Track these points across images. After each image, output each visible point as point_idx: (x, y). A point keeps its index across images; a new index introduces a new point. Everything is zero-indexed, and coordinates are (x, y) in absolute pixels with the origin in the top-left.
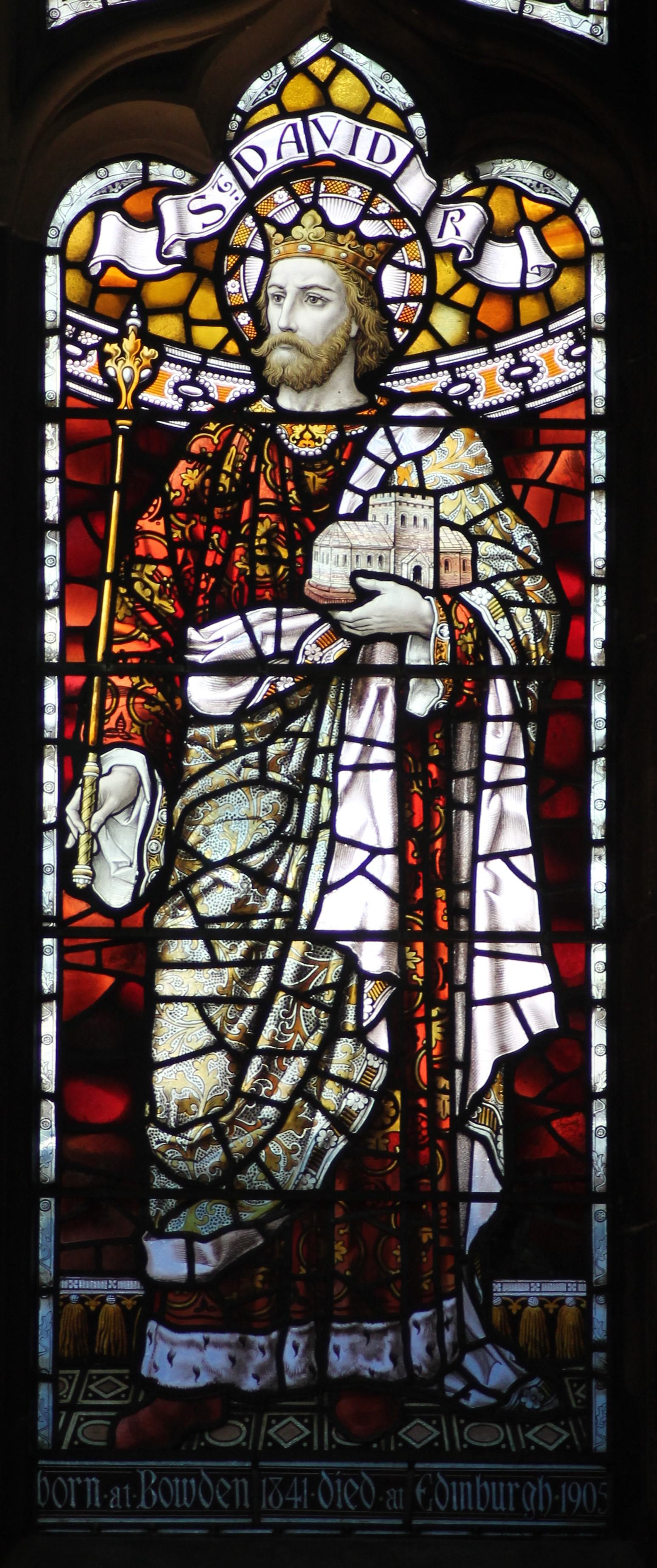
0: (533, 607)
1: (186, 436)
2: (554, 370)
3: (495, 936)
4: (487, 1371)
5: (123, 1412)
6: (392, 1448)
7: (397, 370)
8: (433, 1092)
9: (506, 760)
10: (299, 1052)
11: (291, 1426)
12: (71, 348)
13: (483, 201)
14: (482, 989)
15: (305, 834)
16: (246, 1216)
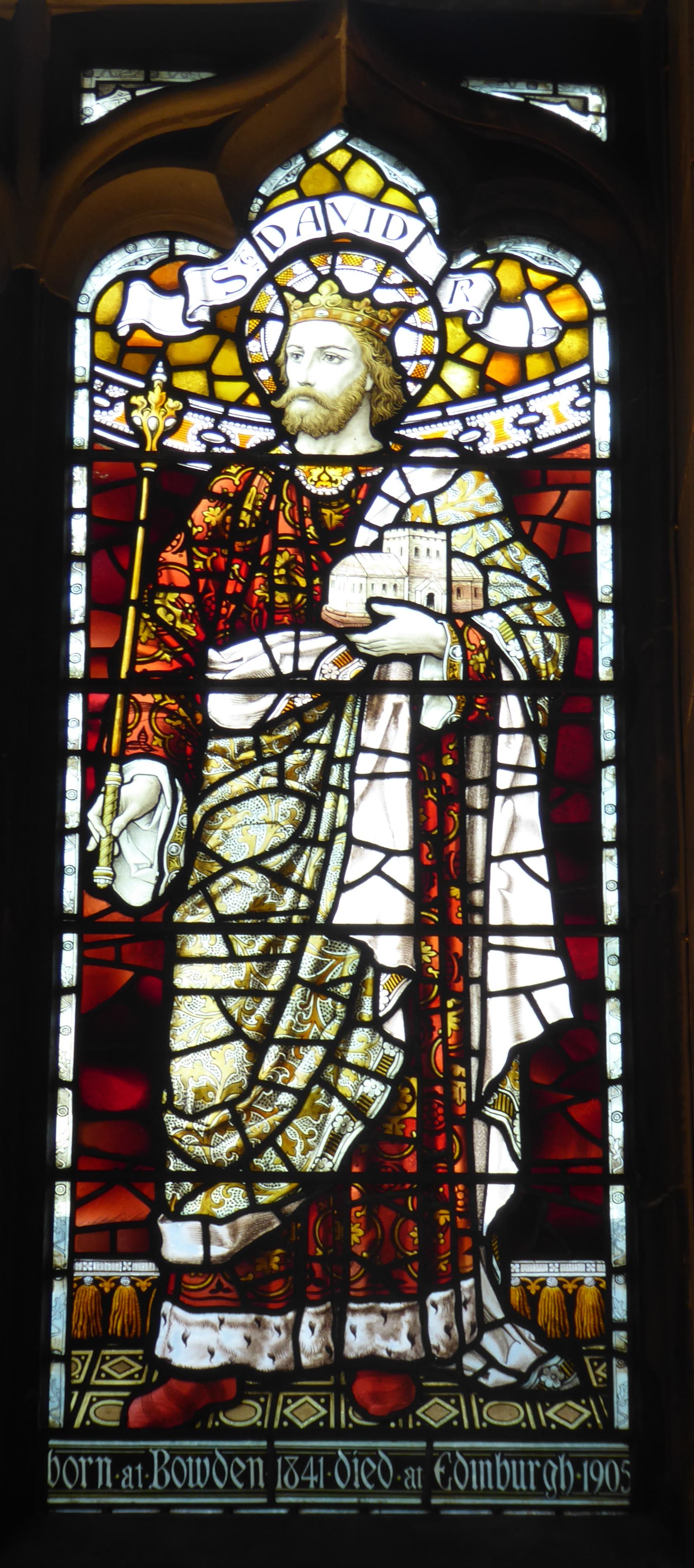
0: (542, 629)
1: (209, 477)
2: (560, 420)
3: (509, 930)
4: (506, 1350)
5: (136, 1392)
6: (411, 1426)
7: (410, 419)
8: (449, 1080)
9: (519, 769)
10: (316, 1042)
11: (307, 1405)
12: (98, 400)
13: (492, 272)
14: (497, 981)
15: (322, 837)
16: (262, 1199)
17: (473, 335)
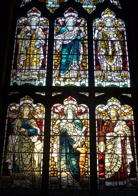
3: (129, 154)
8: (125, 165)
9: (129, 142)
14: (128, 158)
17: (123, 111)
